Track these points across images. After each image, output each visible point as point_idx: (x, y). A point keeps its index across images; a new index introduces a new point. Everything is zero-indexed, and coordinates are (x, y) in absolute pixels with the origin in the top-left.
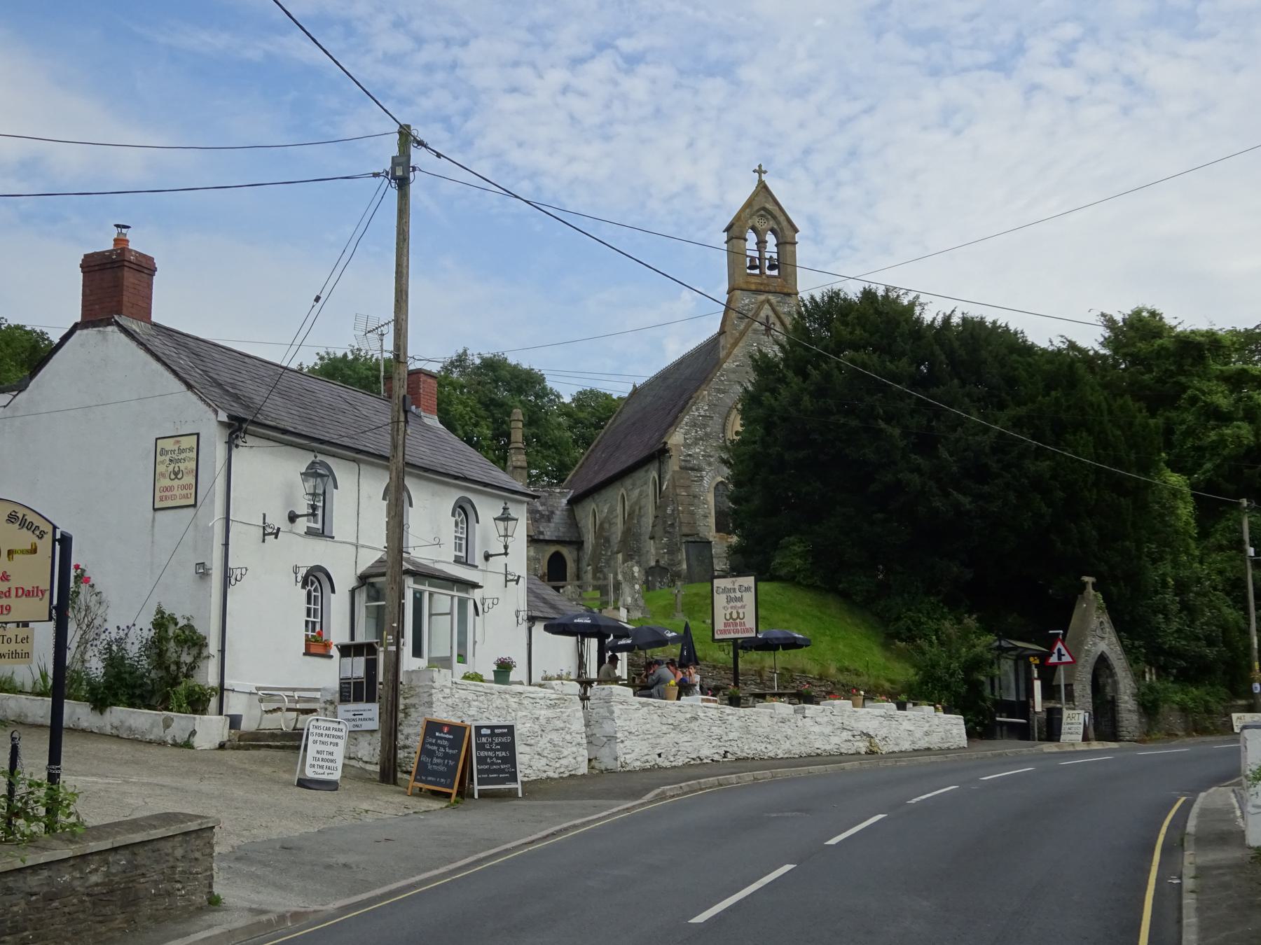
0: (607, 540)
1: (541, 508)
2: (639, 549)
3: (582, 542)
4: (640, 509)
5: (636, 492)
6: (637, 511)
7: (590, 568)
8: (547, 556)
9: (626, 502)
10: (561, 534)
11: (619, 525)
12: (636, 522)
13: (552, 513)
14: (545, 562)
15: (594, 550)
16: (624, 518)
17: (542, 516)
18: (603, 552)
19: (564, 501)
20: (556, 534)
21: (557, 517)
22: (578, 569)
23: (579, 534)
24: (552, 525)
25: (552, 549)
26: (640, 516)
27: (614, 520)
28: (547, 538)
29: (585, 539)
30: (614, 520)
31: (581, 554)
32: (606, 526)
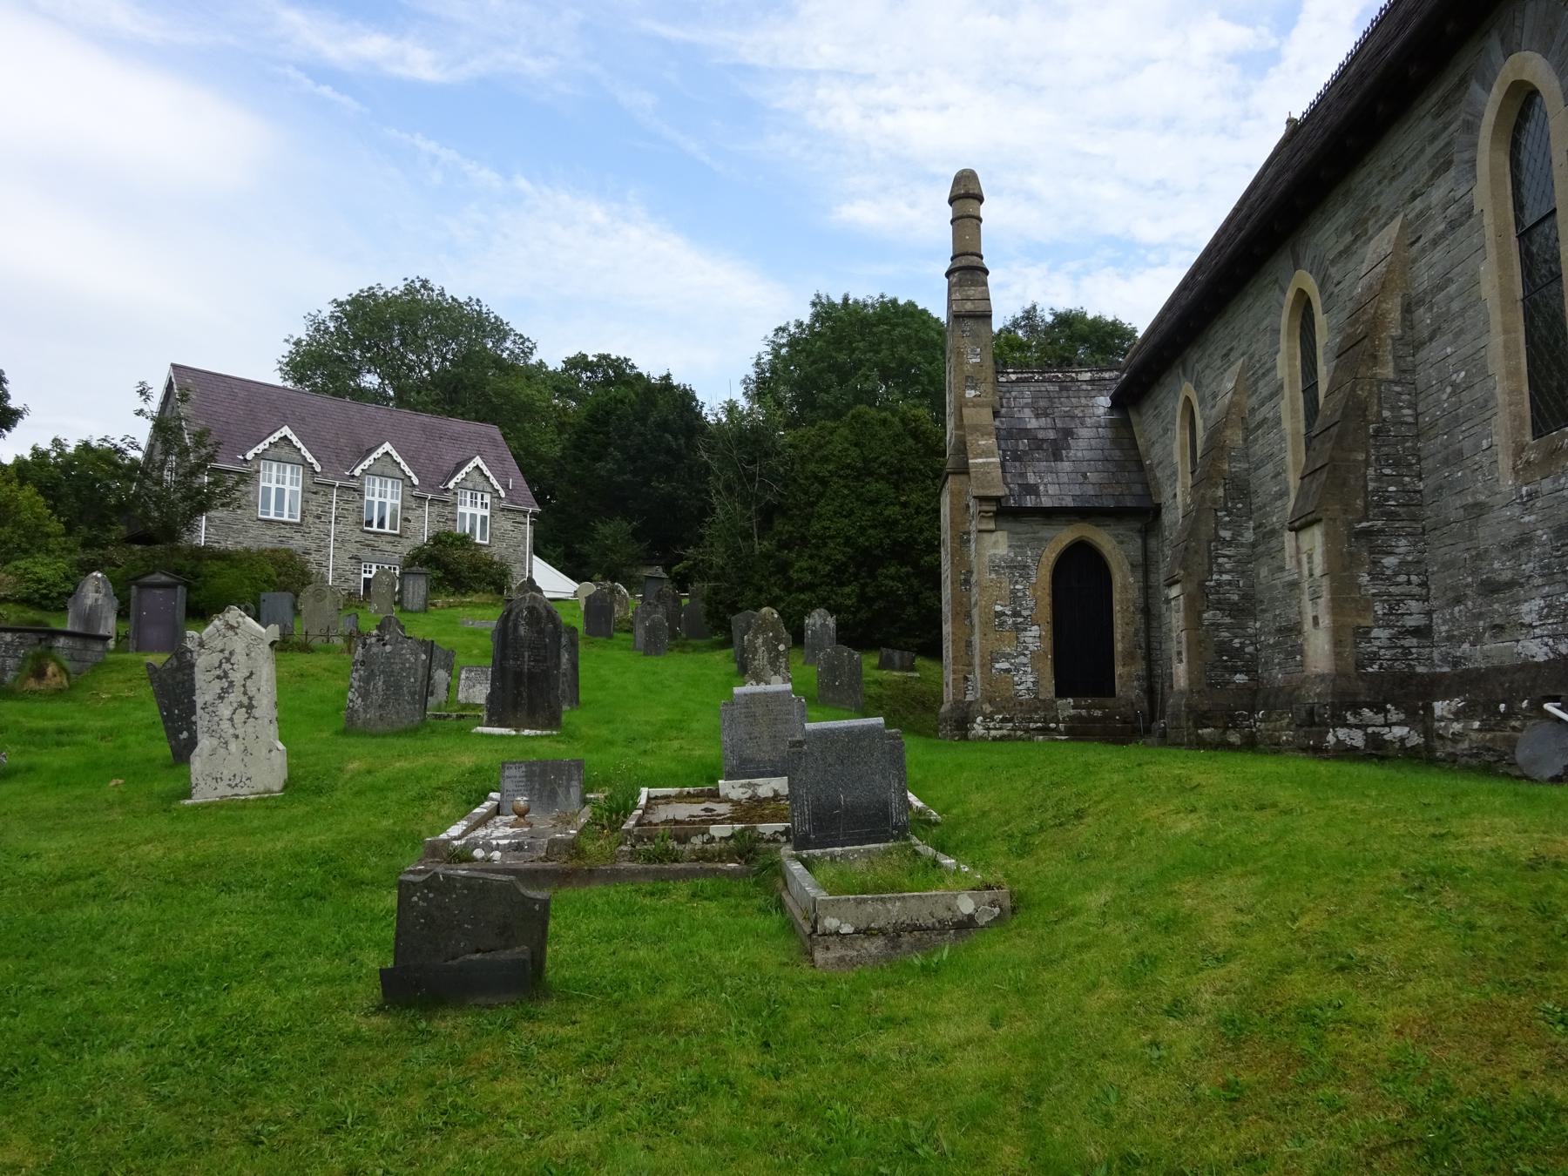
0: (1240, 489)
1: (1033, 424)
2: (1413, 503)
3: (1157, 511)
4: (1408, 309)
5: (1383, 242)
6: (1396, 315)
7: (1175, 591)
8: (1050, 555)
9: (1320, 319)
10: (1090, 490)
11: (1287, 425)
12: (1388, 371)
13: (1068, 433)
14: (1042, 576)
15: (1194, 518)
16: (1310, 389)
17: (1037, 444)
18: (1226, 534)
19: (1104, 401)
21: (1082, 444)
22: (1147, 589)
23: (1146, 485)
24: (1066, 466)
25: (1064, 536)
26: (1411, 343)
27: (1266, 411)
28: (1046, 502)
29: (1165, 498)
30: (1266, 411)
31: (1153, 543)
32: (1234, 436)
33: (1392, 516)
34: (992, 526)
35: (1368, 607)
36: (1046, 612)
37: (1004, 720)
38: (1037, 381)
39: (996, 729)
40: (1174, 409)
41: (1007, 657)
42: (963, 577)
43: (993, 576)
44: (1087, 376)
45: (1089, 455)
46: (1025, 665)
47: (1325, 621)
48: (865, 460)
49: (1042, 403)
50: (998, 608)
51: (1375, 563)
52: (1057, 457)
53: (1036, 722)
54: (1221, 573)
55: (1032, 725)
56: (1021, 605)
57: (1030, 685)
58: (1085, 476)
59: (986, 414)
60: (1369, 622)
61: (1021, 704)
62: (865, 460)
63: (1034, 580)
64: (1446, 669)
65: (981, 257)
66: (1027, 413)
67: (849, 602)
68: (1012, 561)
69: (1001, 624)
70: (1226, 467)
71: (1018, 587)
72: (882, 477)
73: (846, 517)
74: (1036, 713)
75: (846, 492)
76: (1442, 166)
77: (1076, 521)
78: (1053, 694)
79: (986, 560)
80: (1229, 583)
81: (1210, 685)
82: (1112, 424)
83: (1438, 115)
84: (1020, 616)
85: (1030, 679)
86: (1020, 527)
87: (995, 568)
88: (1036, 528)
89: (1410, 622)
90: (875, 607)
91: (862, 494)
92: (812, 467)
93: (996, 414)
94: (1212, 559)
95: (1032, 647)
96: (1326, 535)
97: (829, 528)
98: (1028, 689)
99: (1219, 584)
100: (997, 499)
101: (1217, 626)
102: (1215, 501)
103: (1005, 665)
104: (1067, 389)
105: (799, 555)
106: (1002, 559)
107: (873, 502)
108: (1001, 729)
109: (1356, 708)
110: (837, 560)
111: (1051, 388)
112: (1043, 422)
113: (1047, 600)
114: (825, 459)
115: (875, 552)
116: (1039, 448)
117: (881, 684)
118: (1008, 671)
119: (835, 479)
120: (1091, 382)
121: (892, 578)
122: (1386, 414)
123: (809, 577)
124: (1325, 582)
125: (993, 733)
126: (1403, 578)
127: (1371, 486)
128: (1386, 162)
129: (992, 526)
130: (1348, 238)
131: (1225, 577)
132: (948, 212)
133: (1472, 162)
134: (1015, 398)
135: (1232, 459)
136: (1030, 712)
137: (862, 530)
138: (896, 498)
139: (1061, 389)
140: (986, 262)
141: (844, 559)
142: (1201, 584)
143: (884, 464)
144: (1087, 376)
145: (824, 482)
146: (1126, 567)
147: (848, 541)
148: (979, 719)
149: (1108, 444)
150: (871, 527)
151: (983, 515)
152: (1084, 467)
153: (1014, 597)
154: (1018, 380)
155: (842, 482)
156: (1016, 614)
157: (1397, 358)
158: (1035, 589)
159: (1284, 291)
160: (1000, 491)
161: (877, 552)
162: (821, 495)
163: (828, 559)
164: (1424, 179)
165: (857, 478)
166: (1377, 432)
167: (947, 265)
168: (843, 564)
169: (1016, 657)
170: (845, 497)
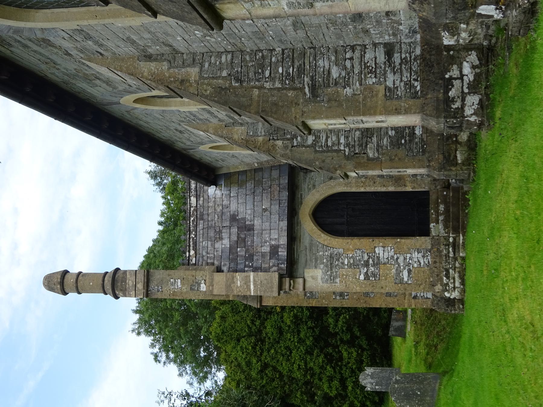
1: (226, 242)
4: (149, 58)
6: (153, 65)
8: (324, 238)
10: (275, 208)
12: (193, 72)
13: (234, 218)
17: (240, 241)
19: (212, 190)
20: (275, 217)
21: (241, 209)
24: (257, 223)
28: (284, 241)
33: (301, 71)
34: (300, 281)
35: (370, 89)
36: (366, 242)
37: (447, 276)
38: (196, 236)
39: (454, 282)
40: (218, 153)
41: (399, 272)
42: (338, 298)
43: (338, 280)
44: (193, 199)
45: (249, 206)
46: (405, 259)
47: (380, 118)
48: (250, 335)
49: (212, 234)
50: (362, 277)
51: (336, 84)
52: (251, 228)
53: (449, 252)
54: (339, 144)
55: (451, 255)
56: (360, 260)
57: (420, 255)
58: (265, 210)
59: (218, 277)
60: (382, 88)
61: (435, 262)
62: (250, 335)
63: (341, 251)
64: (418, 36)
65: (107, 273)
66: (218, 245)
67: (355, 354)
68: (327, 266)
69: (374, 275)
70: (261, 139)
71: (346, 263)
72: (262, 324)
73: (291, 353)
74: (441, 252)
75: (272, 351)
76: (47, 42)
77: (298, 218)
78: (427, 238)
79: (326, 285)
80: (347, 137)
81: (424, 152)
82: (229, 185)
83: (10, 45)
84: (368, 261)
85: (415, 255)
86: (302, 260)
87: (332, 279)
88: (302, 248)
89: (381, 58)
90: (358, 334)
91: (275, 339)
92: (254, 374)
93: (219, 270)
94: (328, 149)
95: (392, 253)
96: (314, 118)
97: (299, 365)
98: (423, 257)
99: (347, 145)
100: (281, 277)
101: (379, 147)
102: (286, 147)
103: (405, 273)
104: (202, 215)
105: (319, 388)
106: (325, 273)
107: (280, 331)
108: (454, 278)
109: (448, 101)
110: (323, 361)
111: (201, 226)
112: (225, 235)
113: (356, 241)
114: (249, 364)
115: (317, 333)
116: (244, 240)
117: (417, 343)
118: (409, 271)
119: (263, 358)
120: (197, 197)
121: (337, 321)
122: (224, 73)
123: (336, 383)
124: (350, 118)
125: (457, 284)
126: (348, 64)
127: (278, 85)
128: (43, 67)
129: (300, 281)
130: (98, 82)
131: (342, 140)
132: (72, 296)
133: (42, 30)
134: (207, 253)
135: (255, 135)
136: (441, 256)
137: (301, 341)
138: (278, 314)
139: (202, 219)
140: (110, 269)
141: (322, 356)
142: (348, 158)
143: (253, 322)
144: (193, 199)
145: (265, 366)
146: (332, 183)
147: (309, 352)
148: (447, 294)
149: (241, 191)
150: (298, 335)
151: (292, 287)
152: (259, 210)
153: (354, 265)
154: (195, 249)
155: (265, 353)
156: (367, 264)
157: (184, 65)
158: (348, 250)
159: (136, 108)
160: (276, 277)
161: (317, 331)
162: (275, 369)
163: (322, 367)
164: (55, 50)
165: (263, 341)
166: (238, 80)
167: (109, 298)
168: (326, 356)
169: (399, 265)
170: (276, 352)
